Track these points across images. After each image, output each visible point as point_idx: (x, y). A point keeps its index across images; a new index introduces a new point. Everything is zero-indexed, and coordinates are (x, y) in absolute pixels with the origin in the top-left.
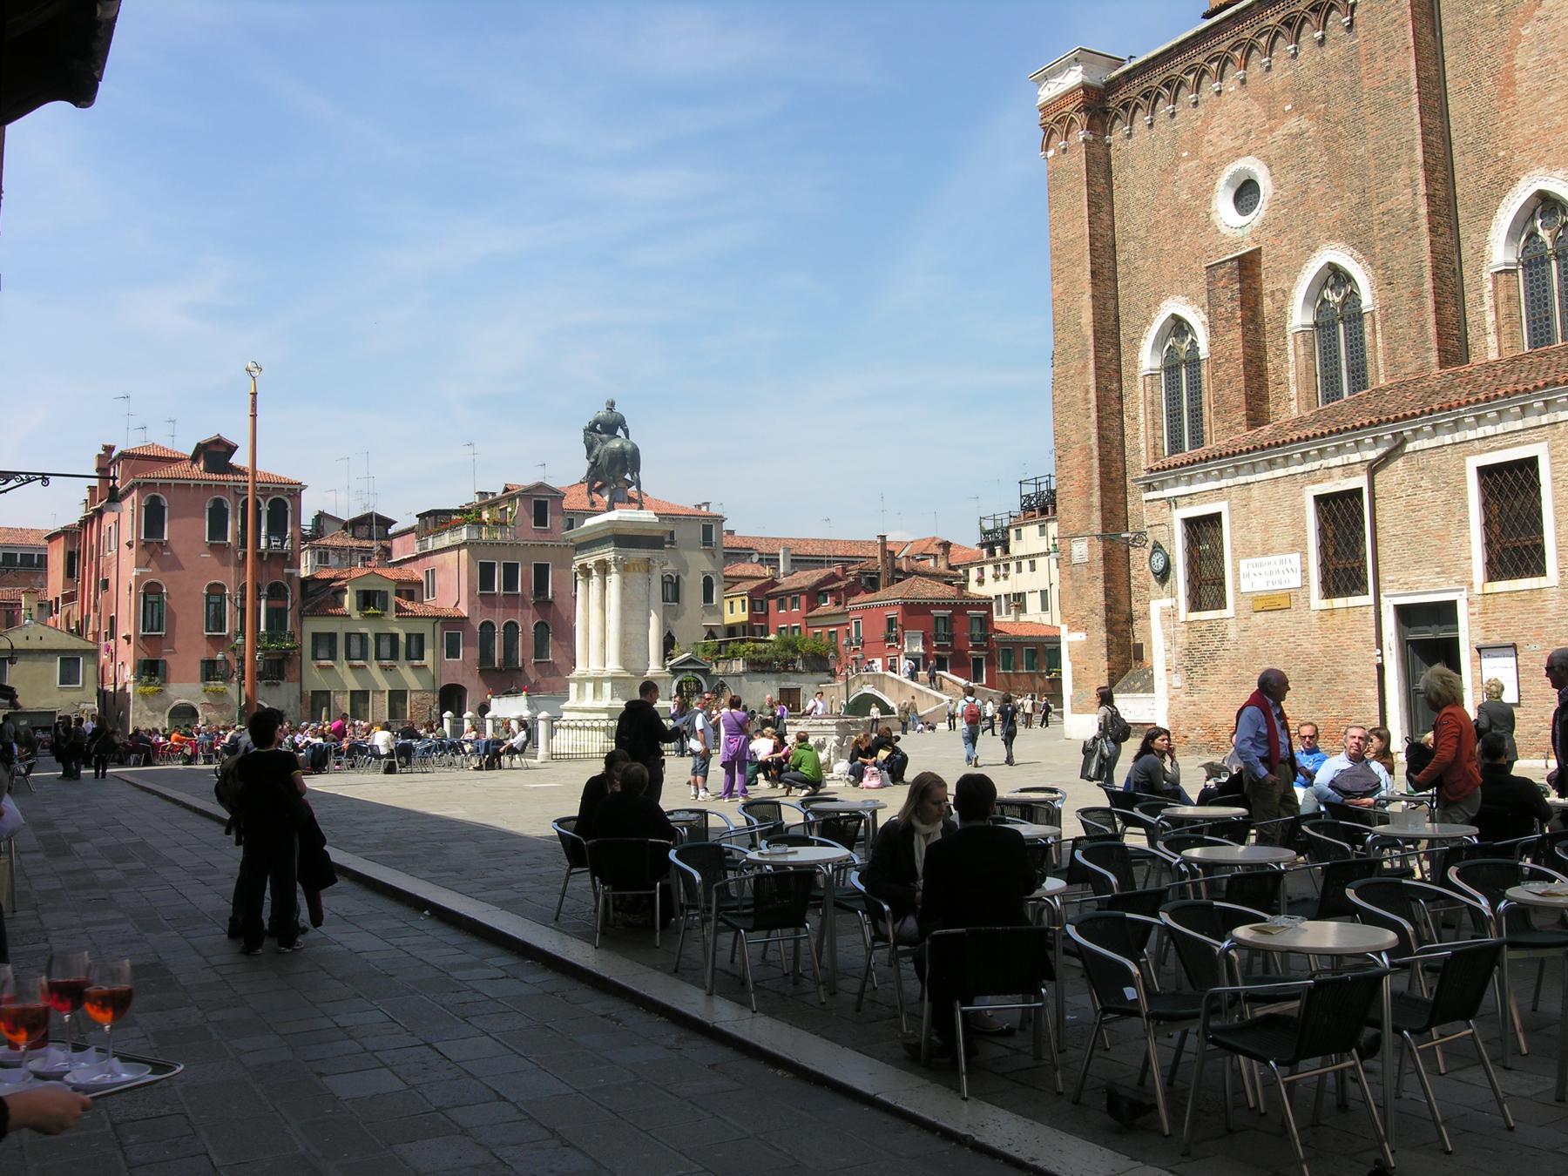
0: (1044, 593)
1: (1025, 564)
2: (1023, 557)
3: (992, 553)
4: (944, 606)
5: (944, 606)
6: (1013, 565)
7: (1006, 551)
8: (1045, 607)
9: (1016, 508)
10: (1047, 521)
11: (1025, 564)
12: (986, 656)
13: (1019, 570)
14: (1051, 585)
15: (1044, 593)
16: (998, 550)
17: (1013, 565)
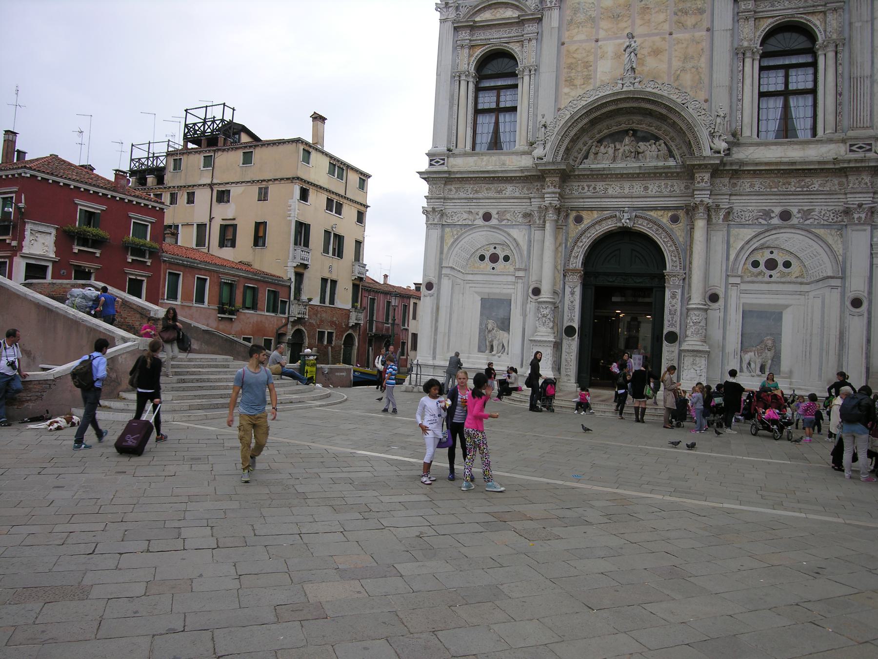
0: (201, 227)
1: (182, 198)
2: (180, 188)
3: (142, 181)
4: (95, 197)
5: (95, 197)
6: (166, 198)
7: (160, 180)
8: (200, 241)
9: (178, 142)
10: (215, 151)
11: (182, 198)
12: (148, 277)
13: (174, 199)
14: (211, 219)
15: (201, 227)
16: (151, 179)
17: (166, 198)
